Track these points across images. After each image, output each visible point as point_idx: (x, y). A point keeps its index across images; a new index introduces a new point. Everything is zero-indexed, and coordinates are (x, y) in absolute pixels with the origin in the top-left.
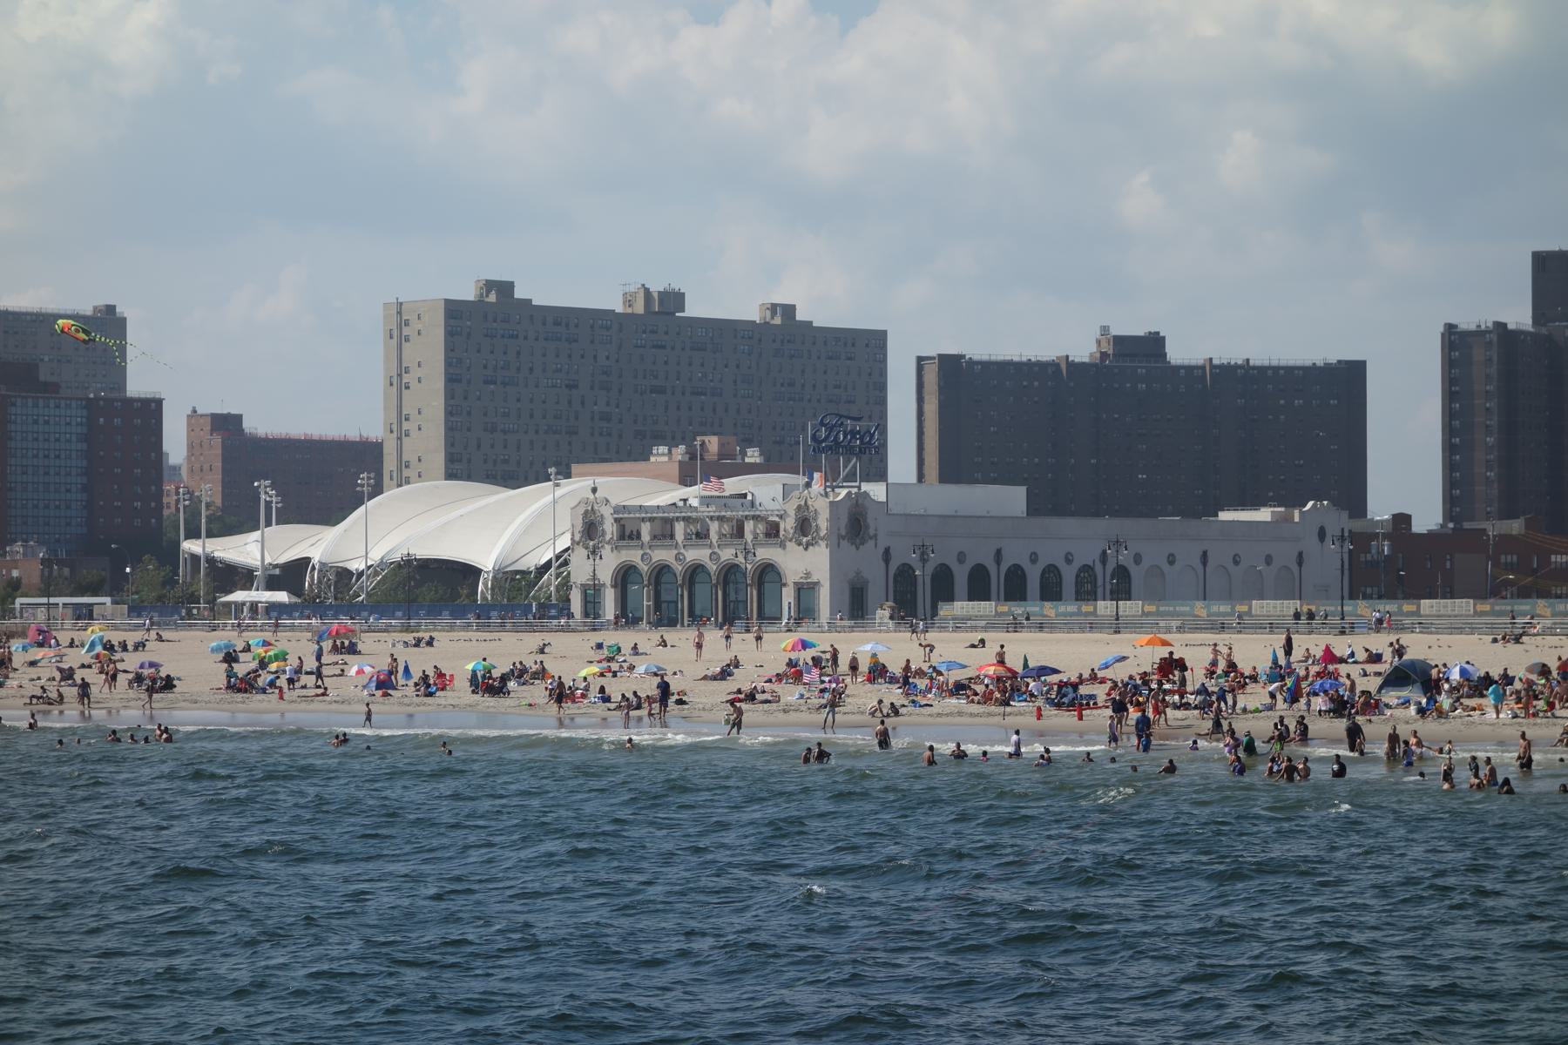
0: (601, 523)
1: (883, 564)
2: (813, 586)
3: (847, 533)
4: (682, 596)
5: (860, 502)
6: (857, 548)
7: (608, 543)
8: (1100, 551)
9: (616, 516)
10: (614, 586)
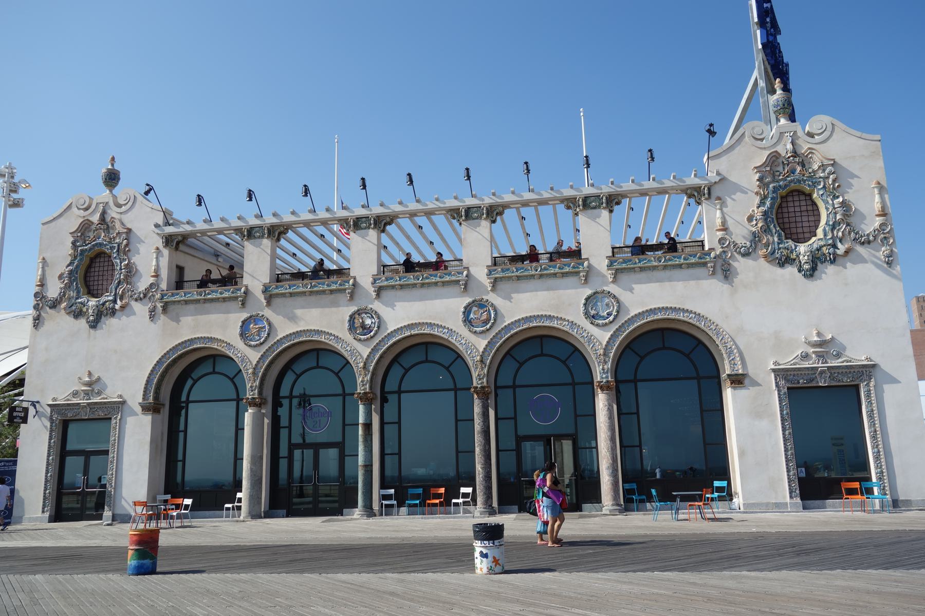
0: (125, 251)
4: (368, 426)
7: (145, 296)
9: (170, 230)
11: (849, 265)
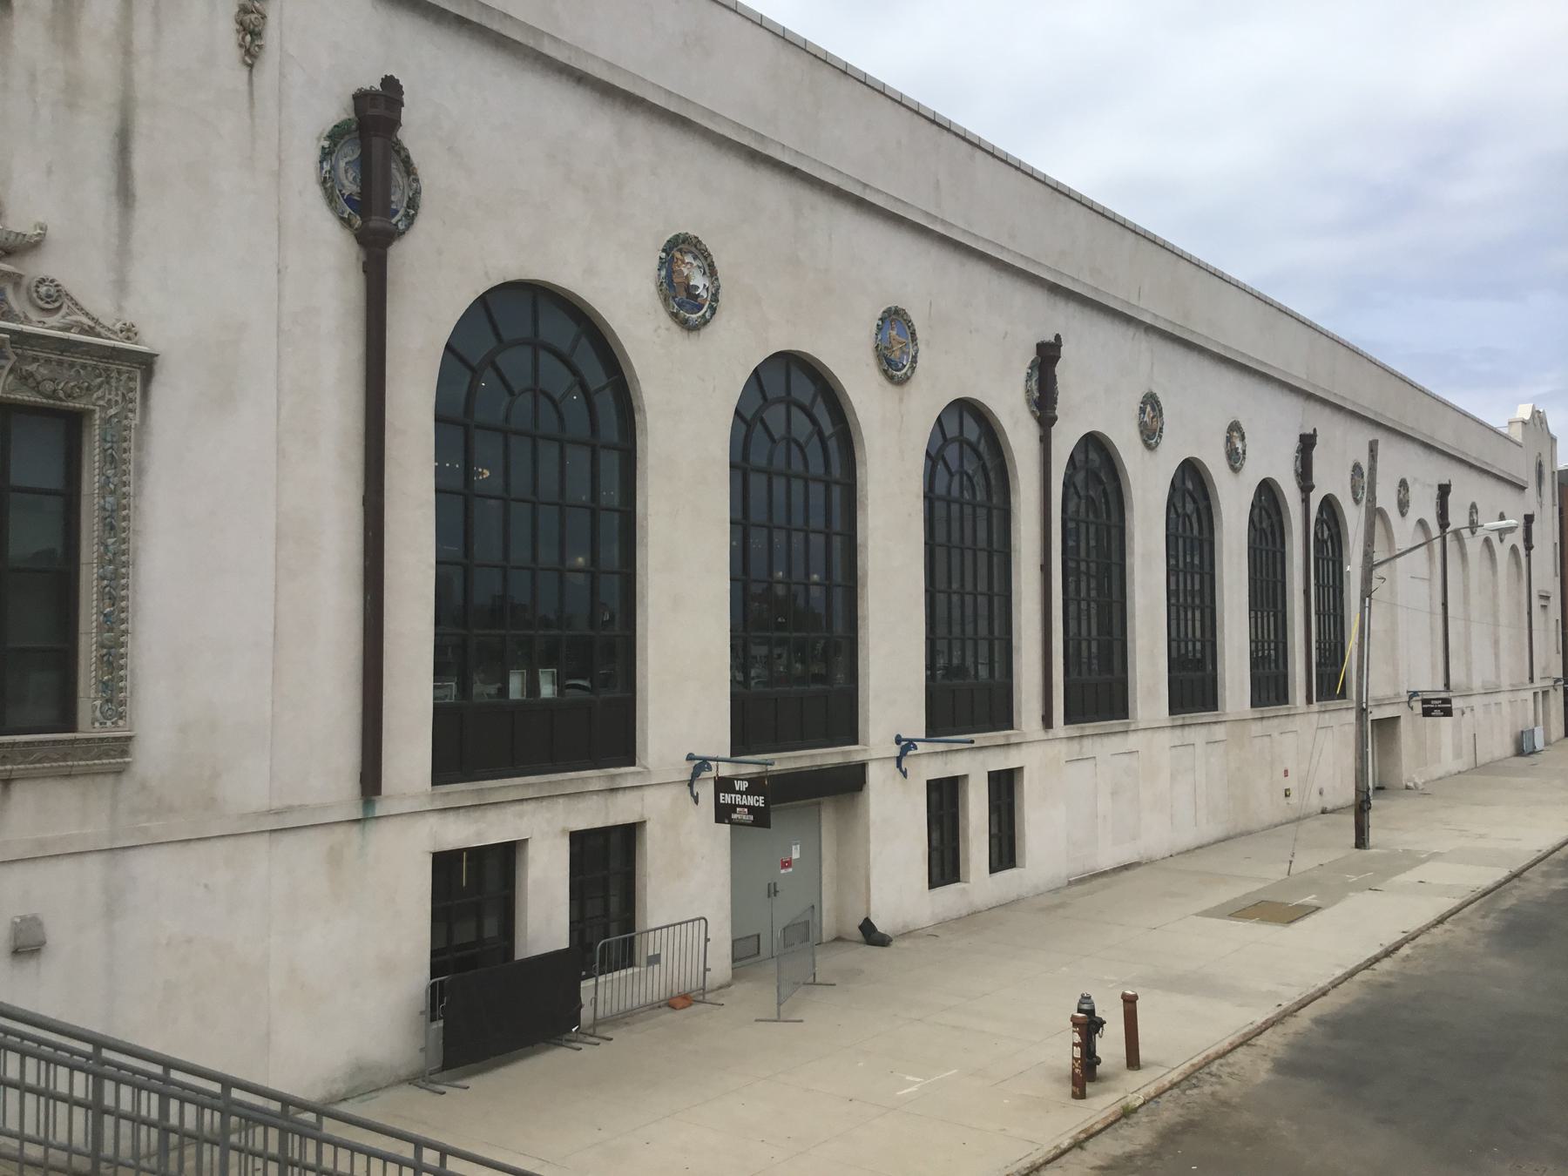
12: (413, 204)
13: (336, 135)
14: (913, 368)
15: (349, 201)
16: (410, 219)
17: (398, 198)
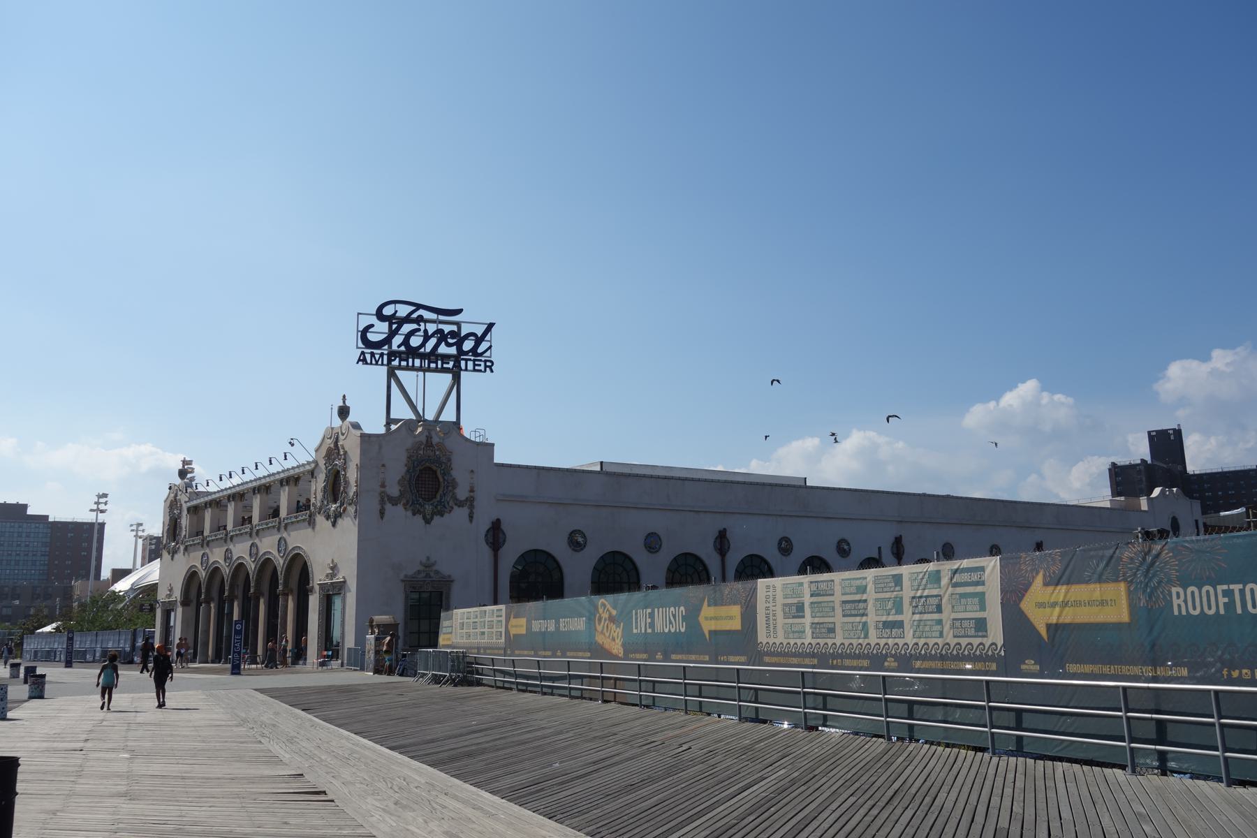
1: (486, 551)
2: (340, 588)
3: (402, 494)
5: (435, 440)
6: (428, 521)
8: (892, 540)
9: (189, 504)
10: (185, 603)
11: (345, 518)
12: (504, 541)
13: (488, 531)
14: (660, 548)
15: (491, 543)
16: (504, 544)
17: (501, 540)
